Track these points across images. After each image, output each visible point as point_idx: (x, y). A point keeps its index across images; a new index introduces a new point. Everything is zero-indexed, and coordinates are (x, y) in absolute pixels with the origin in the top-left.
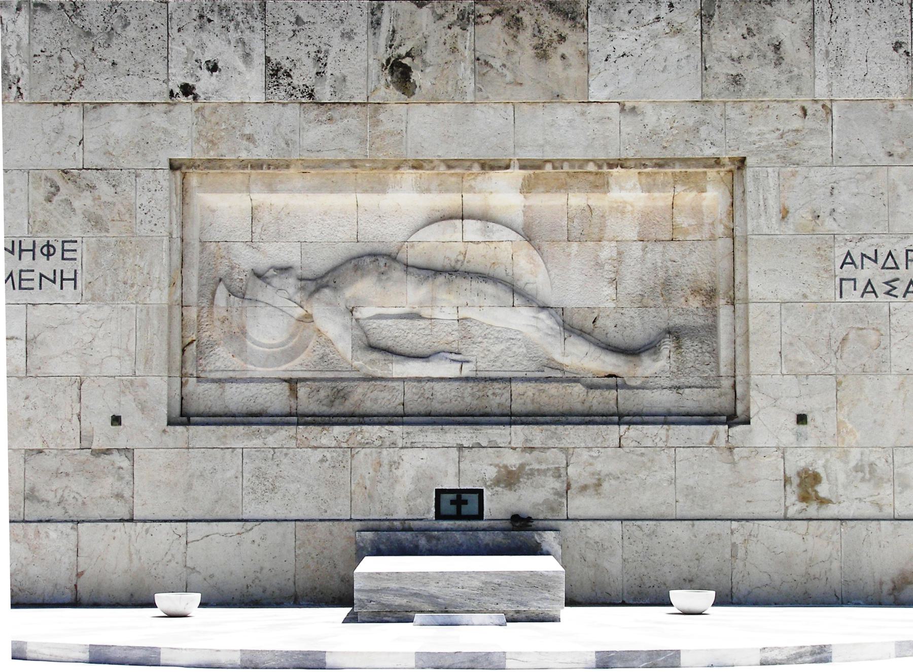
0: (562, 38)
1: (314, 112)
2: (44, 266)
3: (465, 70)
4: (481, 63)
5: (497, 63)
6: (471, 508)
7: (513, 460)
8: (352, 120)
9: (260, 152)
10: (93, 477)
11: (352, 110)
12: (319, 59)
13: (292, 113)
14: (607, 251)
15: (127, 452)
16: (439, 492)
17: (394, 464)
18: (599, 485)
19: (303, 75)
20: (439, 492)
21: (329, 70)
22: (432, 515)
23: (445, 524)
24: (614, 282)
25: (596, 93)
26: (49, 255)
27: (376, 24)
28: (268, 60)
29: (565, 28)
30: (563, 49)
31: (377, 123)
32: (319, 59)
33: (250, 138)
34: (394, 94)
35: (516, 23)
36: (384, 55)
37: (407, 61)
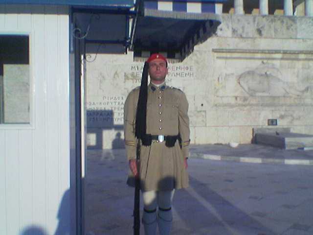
0: (292, 25)
1: (241, 39)
2: (186, 72)
3: (273, 32)
4: (276, 30)
5: (279, 30)
6: (275, 123)
7: (283, 113)
8: (250, 41)
9: (231, 48)
10: (197, 117)
11: (249, 39)
12: (243, 28)
13: (237, 40)
14: (296, 70)
15: (205, 111)
16: (269, 120)
17: (260, 114)
18: (300, 118)
19: (240, 31)
20: (269, 120)
21: (245, 31)
22: (267, 124)
23: (270, 127)
24: (297, 76)
25: (298, 37)
26: (187, 69)
27: (254, 21)
28: (233, 28)
29: (293, 23)
30: (292, 27)
31: (254, 42)
32: (243, 28)
33: (229, 45)
34: (258, 36)
35: (282, 22)
36: (256, 27)
37: (261, 29)
